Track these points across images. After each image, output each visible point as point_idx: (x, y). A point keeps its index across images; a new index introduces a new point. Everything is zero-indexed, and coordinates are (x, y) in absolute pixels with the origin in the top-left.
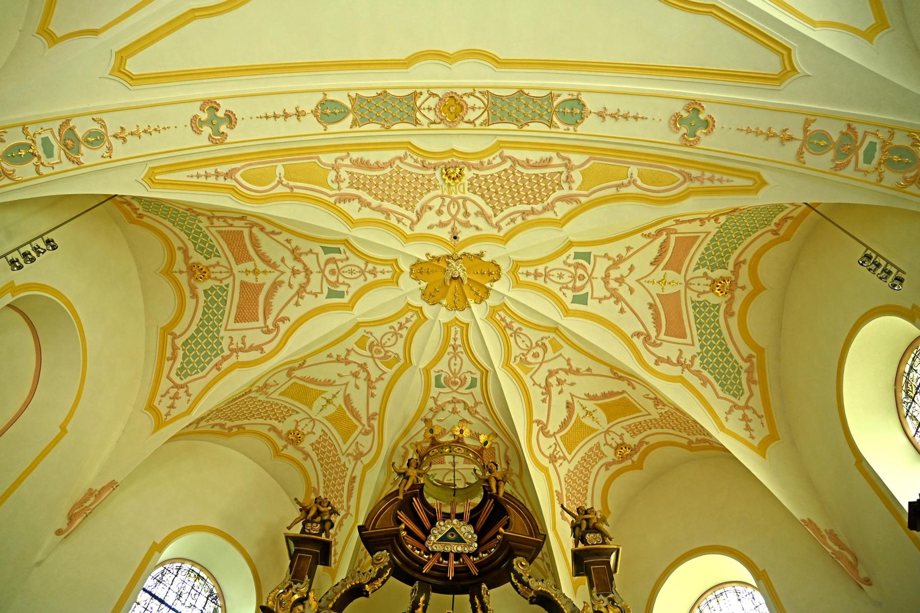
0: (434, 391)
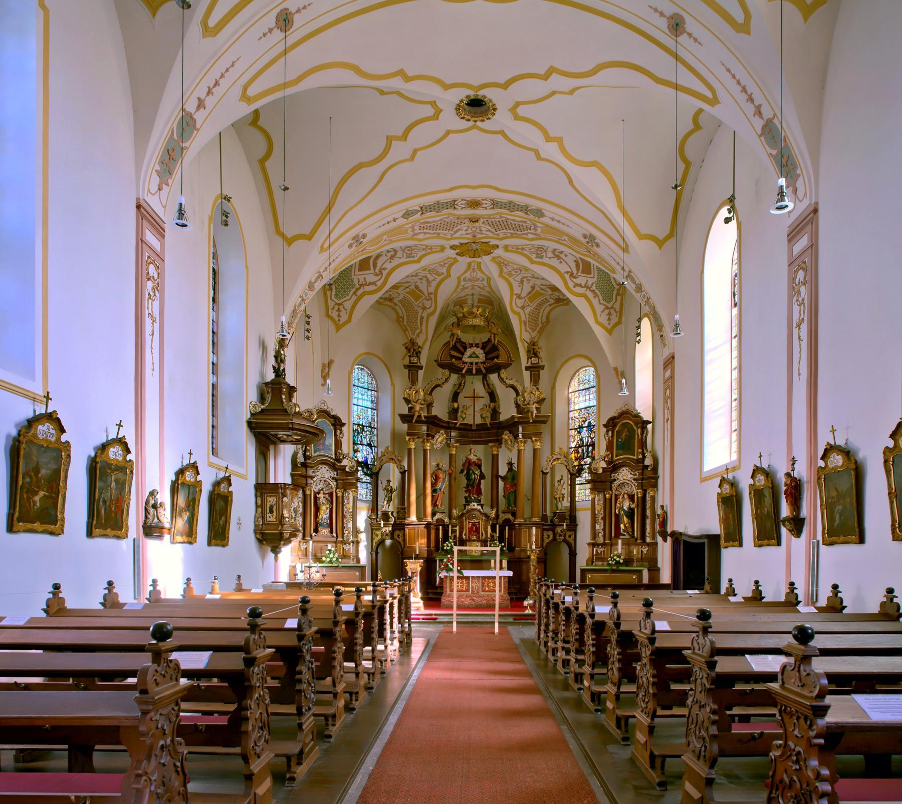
0: (462, 283)
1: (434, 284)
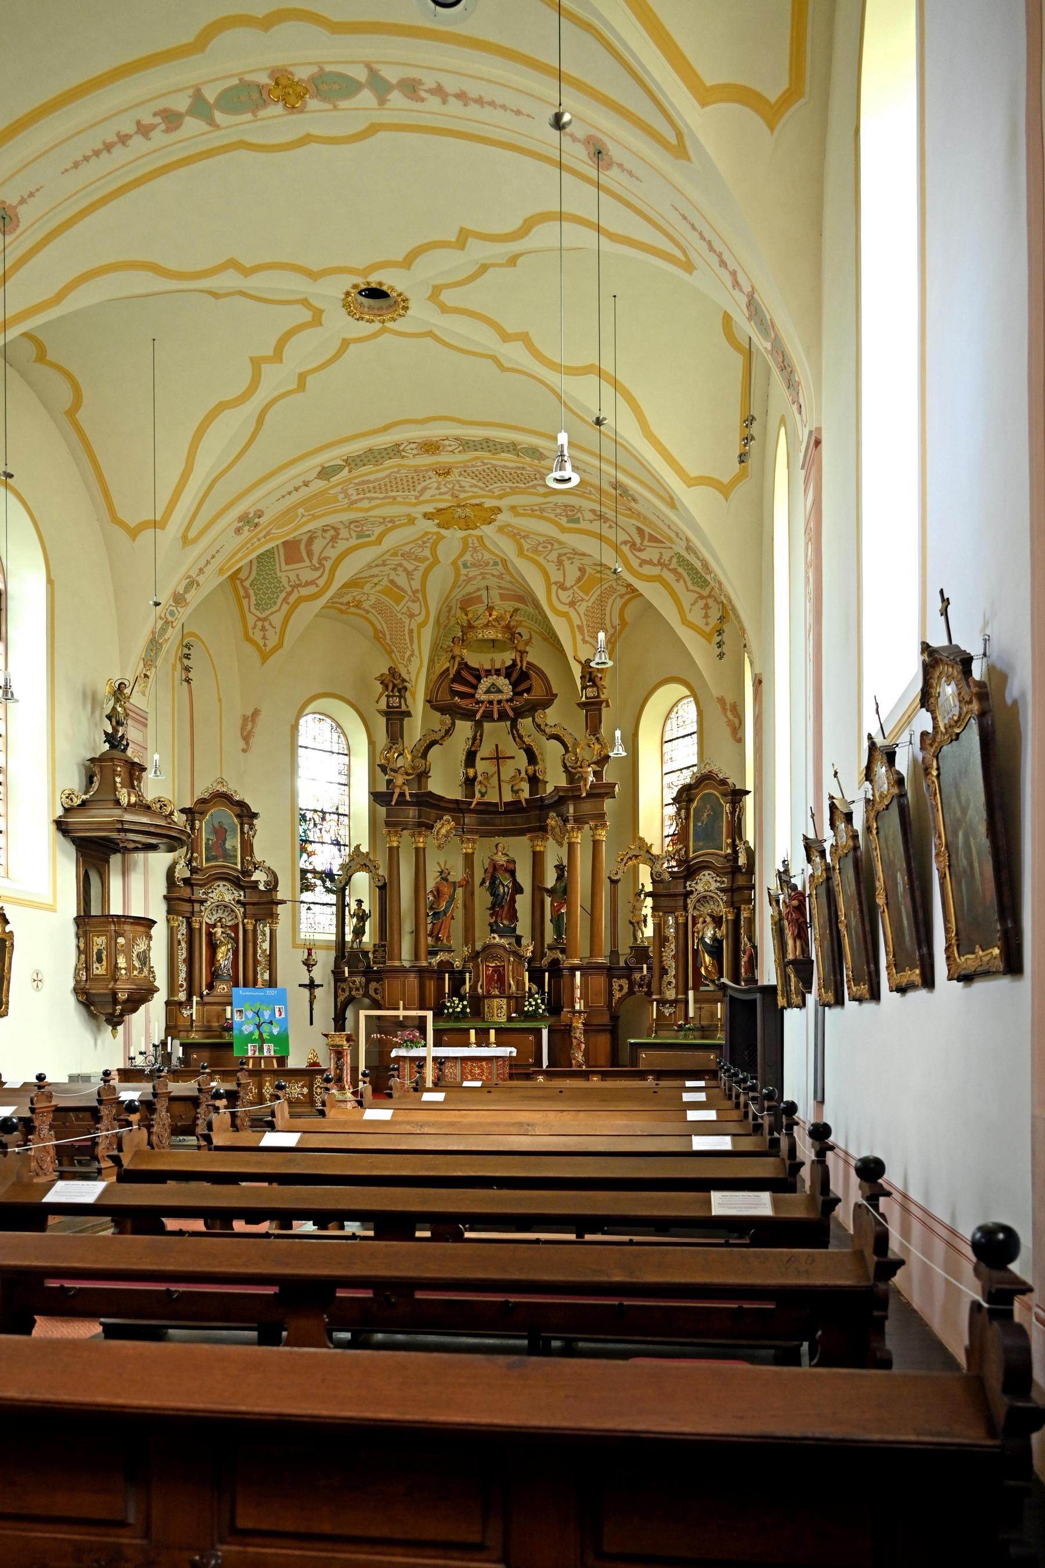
0: (464, 571)
1: (418, 575)
